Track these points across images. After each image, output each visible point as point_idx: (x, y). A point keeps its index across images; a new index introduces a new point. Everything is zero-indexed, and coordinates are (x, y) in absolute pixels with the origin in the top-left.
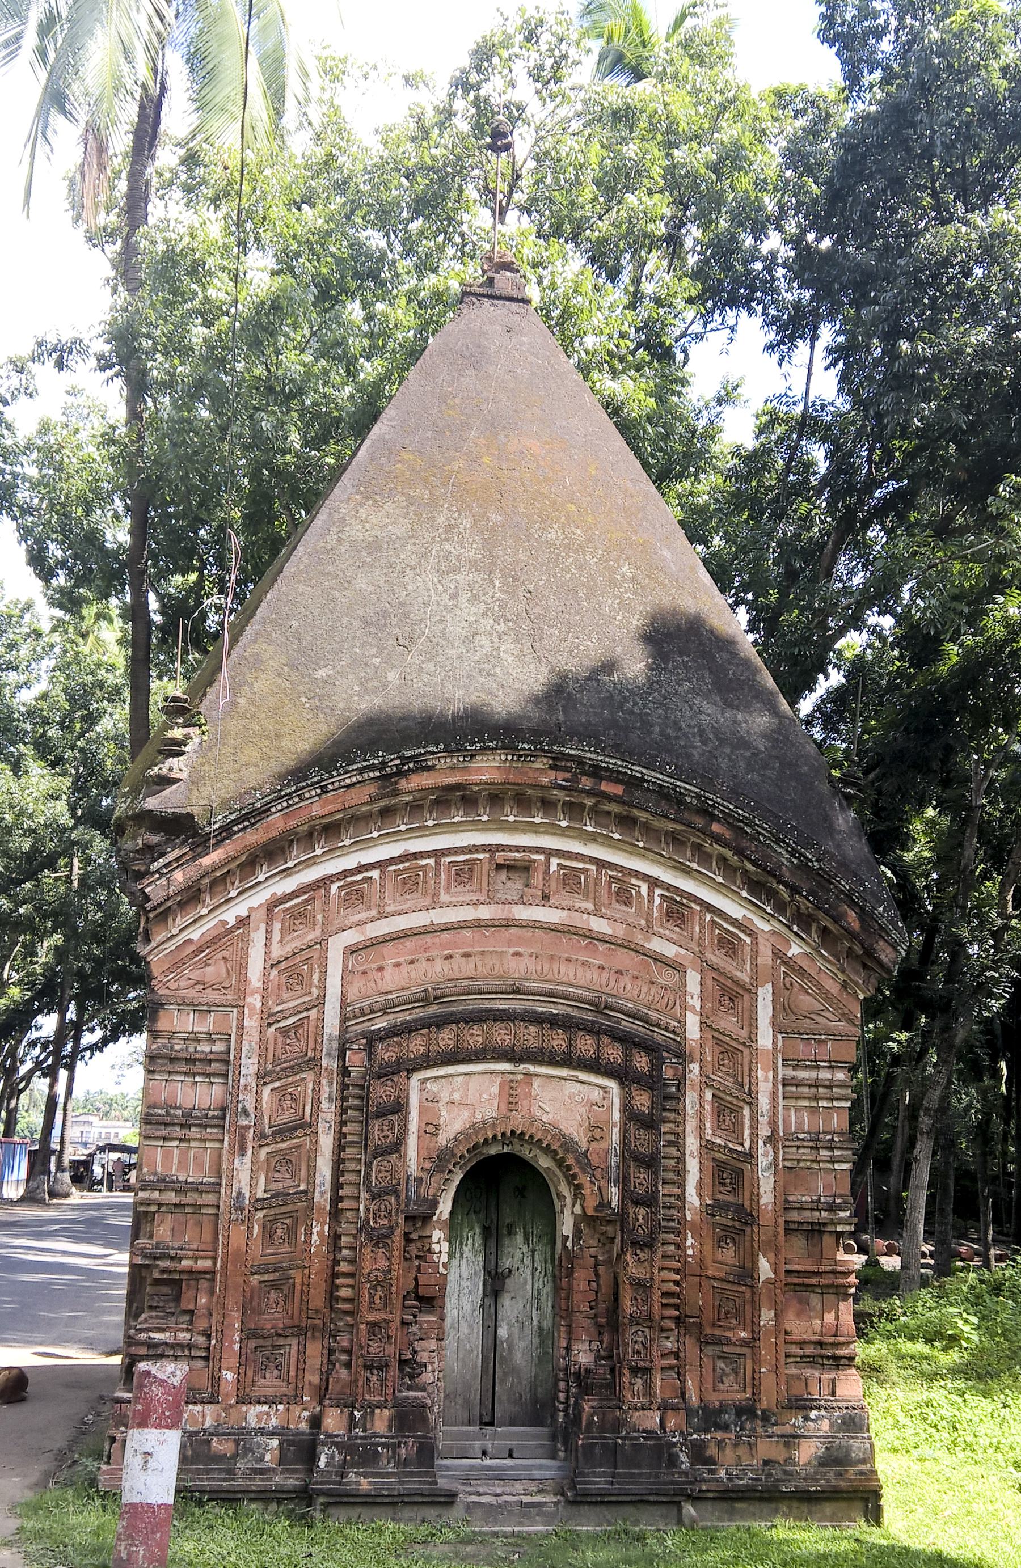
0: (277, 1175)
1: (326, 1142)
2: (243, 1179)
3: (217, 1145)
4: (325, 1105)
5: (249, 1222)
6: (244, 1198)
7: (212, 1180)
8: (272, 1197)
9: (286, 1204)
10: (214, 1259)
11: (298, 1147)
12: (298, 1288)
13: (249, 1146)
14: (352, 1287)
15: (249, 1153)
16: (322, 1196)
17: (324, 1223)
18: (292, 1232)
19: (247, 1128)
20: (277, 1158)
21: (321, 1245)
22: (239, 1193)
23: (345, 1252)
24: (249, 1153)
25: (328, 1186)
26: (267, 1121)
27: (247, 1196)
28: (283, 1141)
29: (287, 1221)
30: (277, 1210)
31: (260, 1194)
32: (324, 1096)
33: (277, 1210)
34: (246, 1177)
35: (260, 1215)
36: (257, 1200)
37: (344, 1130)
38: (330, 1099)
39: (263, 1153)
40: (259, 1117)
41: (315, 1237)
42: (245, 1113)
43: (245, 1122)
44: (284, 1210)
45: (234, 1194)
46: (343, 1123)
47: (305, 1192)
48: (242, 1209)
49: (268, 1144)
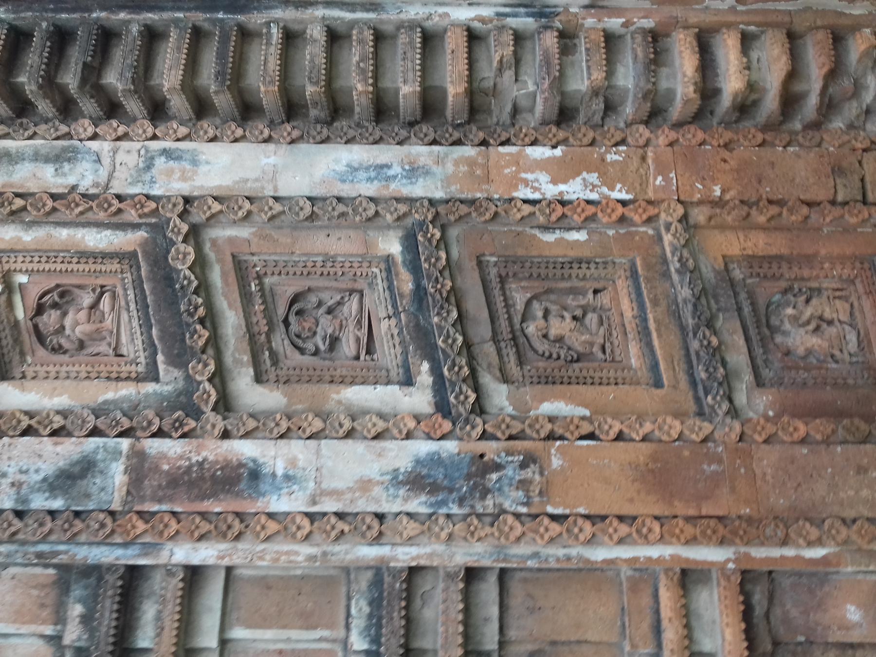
0: (348, 347)
1: (223, 164)
2: (352, 470)
3: (212, 597)
4: (83, 175)
5: (532, 439)
6: (435, 460)
7: (360, 608)
8: (429, 352)
9: (456, 296)
10: (688, 578)
12: (758, 243)
13: (214, 451)
14: (747, 41)
15: (245, 449)
16: (428, 170)
17: (516, 160)
18: (556, 276)
19: (140, 468)
20: (280, 342)
22: (416, 481)
23: (627, 77)
24: (245, 449)
25: (386, 153)
26: (126, 391)
27: (423, 447)
28: (211, 320)
29: (519, 299)
30: (482, 330)
31: (419, 399)
32: (49, 178)
33: (482, 330)
34: (344, 465)
35: (500, 396)
36: (442, 407)
37: (178, 103)
39: (250, 393)
43: (117, 475)
44: (472, 308)
45: (418, 504)
46: (157, 111)
47: (410, 242)
48: (482, 467)
49: (220, 378)
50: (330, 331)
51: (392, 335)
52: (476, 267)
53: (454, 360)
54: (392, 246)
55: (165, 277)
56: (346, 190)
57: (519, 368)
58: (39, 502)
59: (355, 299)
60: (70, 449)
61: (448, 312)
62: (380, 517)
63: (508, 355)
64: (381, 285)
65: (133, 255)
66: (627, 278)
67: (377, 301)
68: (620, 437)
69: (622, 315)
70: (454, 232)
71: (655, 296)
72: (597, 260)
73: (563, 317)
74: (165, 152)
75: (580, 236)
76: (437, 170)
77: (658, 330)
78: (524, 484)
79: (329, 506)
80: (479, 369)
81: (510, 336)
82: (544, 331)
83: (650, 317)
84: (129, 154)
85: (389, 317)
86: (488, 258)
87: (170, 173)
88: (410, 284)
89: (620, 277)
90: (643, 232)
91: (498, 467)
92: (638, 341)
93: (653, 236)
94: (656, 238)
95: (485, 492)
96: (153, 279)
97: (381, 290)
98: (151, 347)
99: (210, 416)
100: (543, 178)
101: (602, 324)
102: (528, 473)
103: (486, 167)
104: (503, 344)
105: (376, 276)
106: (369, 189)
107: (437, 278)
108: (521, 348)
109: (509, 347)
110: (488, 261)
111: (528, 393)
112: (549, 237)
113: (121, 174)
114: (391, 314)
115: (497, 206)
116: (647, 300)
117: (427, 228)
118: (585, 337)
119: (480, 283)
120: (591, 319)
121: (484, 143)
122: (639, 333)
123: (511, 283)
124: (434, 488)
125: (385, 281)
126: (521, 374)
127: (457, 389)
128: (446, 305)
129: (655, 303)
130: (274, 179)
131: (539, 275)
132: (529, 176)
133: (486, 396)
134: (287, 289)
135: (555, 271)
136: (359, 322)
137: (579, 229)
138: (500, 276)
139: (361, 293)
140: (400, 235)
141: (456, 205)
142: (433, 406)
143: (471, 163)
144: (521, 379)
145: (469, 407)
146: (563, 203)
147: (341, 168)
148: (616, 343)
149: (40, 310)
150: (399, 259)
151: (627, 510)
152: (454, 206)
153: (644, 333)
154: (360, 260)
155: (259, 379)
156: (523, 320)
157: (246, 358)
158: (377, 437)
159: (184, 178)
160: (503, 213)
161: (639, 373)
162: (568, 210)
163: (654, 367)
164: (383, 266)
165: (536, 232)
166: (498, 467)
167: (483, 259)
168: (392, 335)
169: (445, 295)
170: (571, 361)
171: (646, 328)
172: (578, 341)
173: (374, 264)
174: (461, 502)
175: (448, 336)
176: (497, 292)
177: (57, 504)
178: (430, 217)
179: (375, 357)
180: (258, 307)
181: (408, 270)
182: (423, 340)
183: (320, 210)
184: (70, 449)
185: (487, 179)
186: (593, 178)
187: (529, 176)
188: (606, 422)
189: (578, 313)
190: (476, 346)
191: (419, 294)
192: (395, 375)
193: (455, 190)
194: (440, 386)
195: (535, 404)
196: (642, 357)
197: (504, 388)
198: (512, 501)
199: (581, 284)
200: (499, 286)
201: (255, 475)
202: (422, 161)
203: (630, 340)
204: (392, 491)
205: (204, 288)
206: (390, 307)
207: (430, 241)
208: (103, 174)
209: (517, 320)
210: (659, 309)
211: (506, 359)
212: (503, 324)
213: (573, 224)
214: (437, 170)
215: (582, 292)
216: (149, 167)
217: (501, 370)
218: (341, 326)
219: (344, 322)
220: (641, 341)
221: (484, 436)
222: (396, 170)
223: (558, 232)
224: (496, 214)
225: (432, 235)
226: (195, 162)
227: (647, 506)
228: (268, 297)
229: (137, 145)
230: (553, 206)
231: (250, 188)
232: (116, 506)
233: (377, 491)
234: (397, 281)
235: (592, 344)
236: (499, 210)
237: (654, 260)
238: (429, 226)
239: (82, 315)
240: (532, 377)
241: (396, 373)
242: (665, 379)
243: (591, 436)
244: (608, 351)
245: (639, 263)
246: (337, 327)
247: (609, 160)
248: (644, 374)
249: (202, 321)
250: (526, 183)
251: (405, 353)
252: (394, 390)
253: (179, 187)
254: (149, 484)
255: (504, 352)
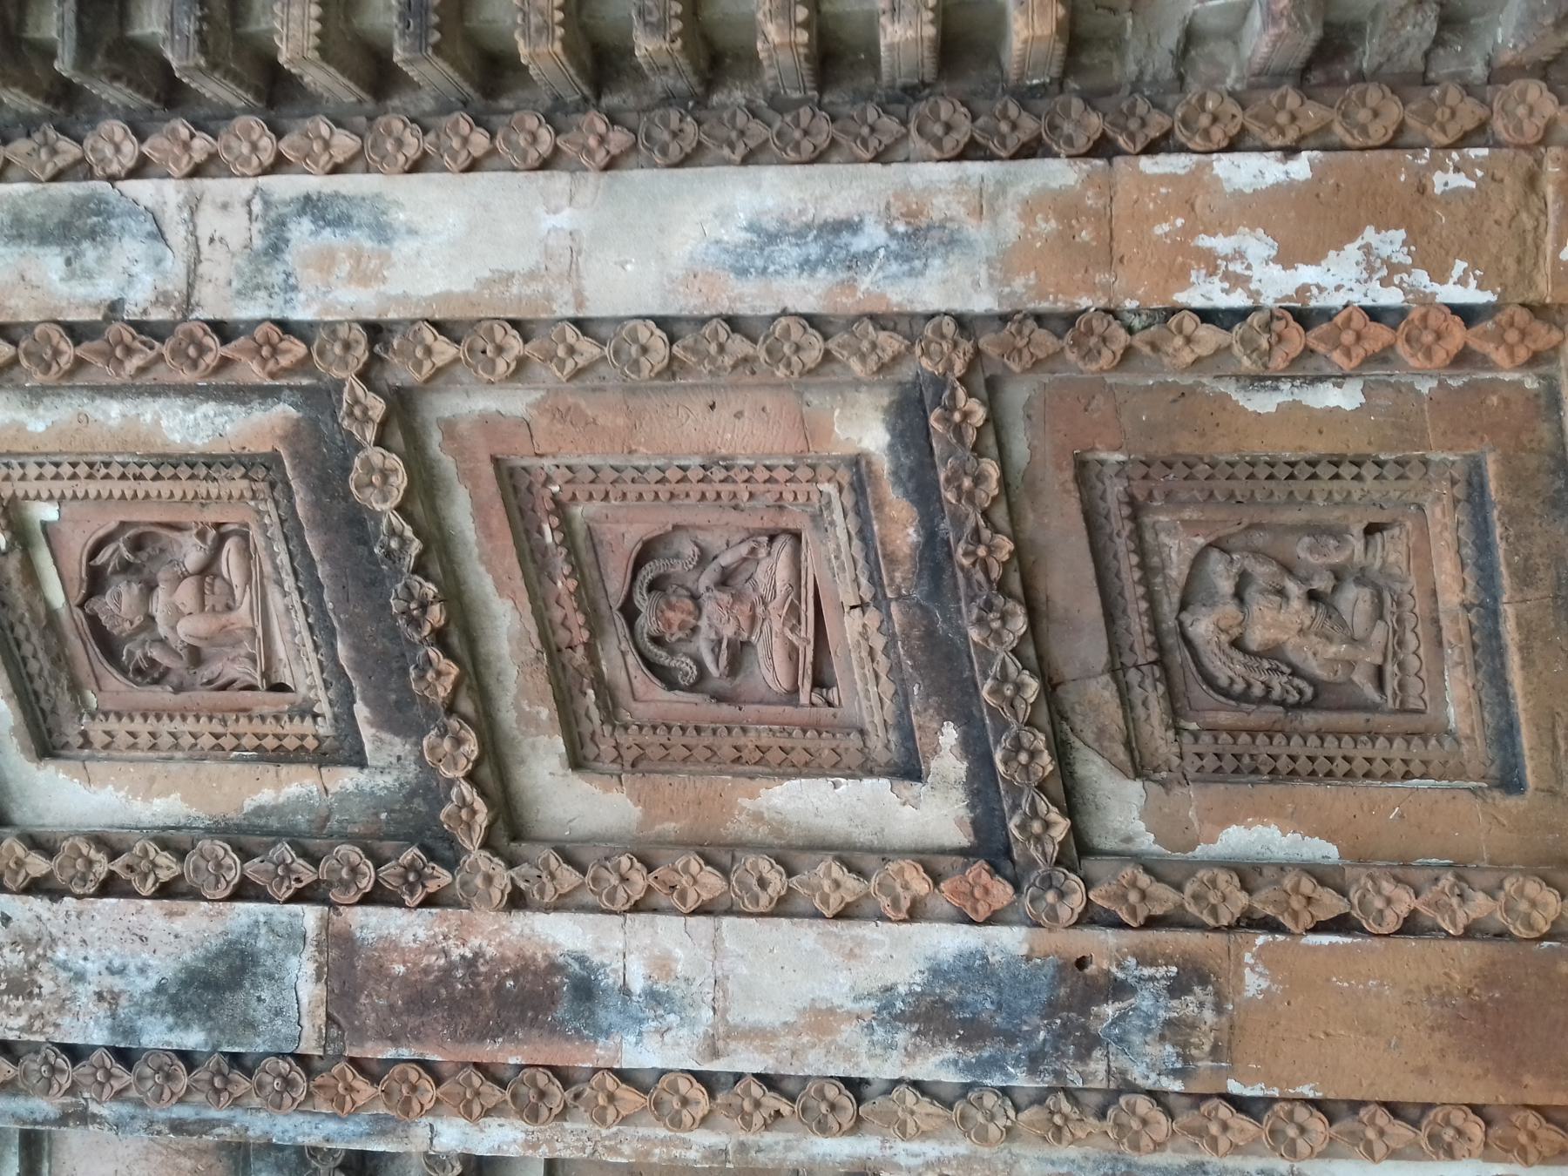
0: (771, 668)
1: (451, 234)
4: (128, 275)
6: (974, 969)
8: (958, 701)
9: (1024, 583)
11: (512, 483)
13: (497, 935)
15: (561, 934)
16: (954, 234)
19: (345, 966)
20: (619, 662)
21: (1413, 210)
22: (933, 1013)
24: (561, 934)
25: (849, 190)
26: (293, 788)
27: (948, 941)
28: (461, 635)
31: (936, 813)
33: (1082, 648)
35: (1124, 810)
36: (990, 847)
38: (74, 230)
40: (255, 859)
41: (1338, 279)
42: (215, 983)
43: (304, 980)
45: (938, 1065)
46: (276, 91)
47: (910, 414)
48: (1082, 987)
49: (494, 772)
50: (728, 632)
51: (871, 651)
52: (1071, 486)
53: (1017, 738)
54: (867, 432)
55: (354, 525)
56: (750, 297)
57: (1171, 734)
58: (157, 1034)
59: (783, 549)
60: (196, 929)
61: (1004, 618)
62: (855, 1086)
63: (1145, 703)
64: (842, 526)
65: (271, 462)
66: (1456, 502)
67: (833, 557)
68: (1411, 926)
69: (1434, 593)
70: (1018, 394)
71: (1526, 559)
72: (1382, 457)
73: (1281, 592)
74: (309, 205)
75: (1342, 398)
76: (977, 231)
77: (1524, 649)
78: (1176, 1030)
79: (746, 1060)
80: (1078, 744)
81: (1152, 656)
82: (1235, 632)
83: (1508, 611)
84: (227, 212)
85: (862, 606)
86: (1103, 455)
87: (326, 261)
88: (911, 531)
89: (1438, 498)
90: (1511, 383)
91: (1119, 989)
92: (1471, 669)
93: (1537, 396)
94: (1542, 401)
95: (1088, 1044)
96: (324, 524)
97: (843, 538)
98: (334, 674)
99: (477, 857)
100: (1257, 246)
101: (1381, 617)
102: (1187, 1006)
103: (1105, 220)
104: (1133, 676)
105: (829, 503)
106: (806, 293)
107: (976, 531)
108: (1178, 678)
109: (1148, 682)
110: (1102, 463)
111: (1191, 801)
112: (1263, 403)
113: (217, 267)
114: (867, 598)
115: (1130, 330)
116: (1503, 569)
117: (953, 397)
118: (1338, 649)
119: (1081, 525)
120: (1354, 601)
121: (1102, 148)
122: (1474, 647)
123: (1158, 510)
124: (972, 1032)
125: (851, 515)
126: (1175, 749)
127: (1026, 807)
128: (999, 601)
129: (1525, 576)
130: (572, 272)
131: (1232, 495)
132: (1220, 244)
133: (1092, 808)
134: (626, 531)
135: (1272, 484)
136: (794, 610)
137: (1340, 379)
138: (1132, 501)
139: (797, 536)
140: (885, 401)
141: (1026, 331)
142: (970, 830)
143: (1066, 207)
144: (1176, 761)
145: (1052, 850)
146: (1304, 317)
147: (735, 234)
148: (1413, 663)
149: (96, 581)
150: (884, 465)
151: (1410, 1091)
152: (1020, 332)
153: (1487, 650)
154: (790, 462)
155: (577, 761)
156: (1184, 606)
157: (546, 712)
158: (845, 914)
159: (362, 276)
160: (1147, 350)
161: (1465, 748)
162: (1320, 339)
163: (1505, 734)
164: (845, 476)
165: (1230, 389)
166: (1119, 989)
167: (1089, 456)
168: (871, 651)
169: (996, 573)
170: (1298, 706)
171: (1495, 635)
172: (1319, 657)
173: (824, 472)
174: (1034, 1063)
175: (1004, 678)
176: (1122, 544)
177: (193, 1039)
178: (959, 368)
179: (833, 695)
180: (564, 585)
181: (906, 494)
182: (943, 670)
183: (690, 344)
184: (196, 929)
185: (1109, 256)
186: (1391, 243)
187: (1220, 244)
188: (1379, 892)
189: (1322, 584)
190: (1070, 686)
191: (934, 556)
192: (880, 746)
193: (1025, 291)
194: (983, 785)
195: (1208, 827)
196: (1475, 708)
197: (1136, 787)
198: (1148, 1062)
199: (1337, 513)
200: (1129, 526)
201: (586, 989)
202: (941, 206)
203: (1448, 663)
204: (880, 1033)
205: (438, 550)
206: (864, 581)
207: (958, 430)
208: (175, 266)
209: (1169, 606)
210: (1531, 594)
211: (1140, 711)
212: (1136, 624)
213: (1328, 371)
214: (977, 231)
215: (1338, 533)
216: (276, 248)
217: (1128, 744)
218: (753, 619)
219: (760, 610)
220: (1477, 666)
221: (1090, 917)
222: (873, 236)
223: (1285, 386)
224: (1129, 351)
225: (966, 415)
226: (382, 231)
227: (1456, 1084)
228: (581, 550)
229: (240, 188)
230: (1278, 326)
231: (518, 299)
232: (309, 1046)
233: (848, 1033)
234: (880, 521)
235: (1351, 665)
236: (1138, 341)
237: (1533, 462)
238: (954, 383)
239: (186, 593)
240: (1200, 756)
241: (882, 744)
242: (1528, 771)
243: (1341, 924)
244: (1391, 684)
245: (1491, 469)
246: (745, 624)
247: (1438, 190)
248: (1477, 752)
249: (440, 638)
250: (1210, 262)
251: (903, 697)
252: (878, 788)
253: (352, 300)
254: (371, 1004)
255: (1137, 694)
